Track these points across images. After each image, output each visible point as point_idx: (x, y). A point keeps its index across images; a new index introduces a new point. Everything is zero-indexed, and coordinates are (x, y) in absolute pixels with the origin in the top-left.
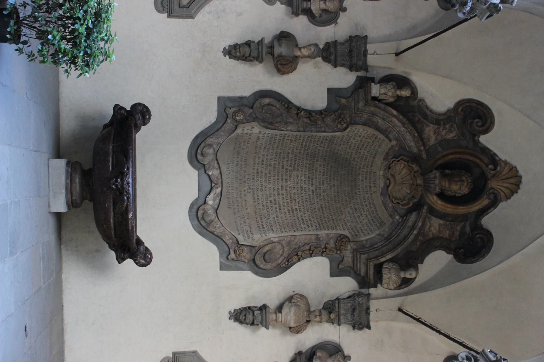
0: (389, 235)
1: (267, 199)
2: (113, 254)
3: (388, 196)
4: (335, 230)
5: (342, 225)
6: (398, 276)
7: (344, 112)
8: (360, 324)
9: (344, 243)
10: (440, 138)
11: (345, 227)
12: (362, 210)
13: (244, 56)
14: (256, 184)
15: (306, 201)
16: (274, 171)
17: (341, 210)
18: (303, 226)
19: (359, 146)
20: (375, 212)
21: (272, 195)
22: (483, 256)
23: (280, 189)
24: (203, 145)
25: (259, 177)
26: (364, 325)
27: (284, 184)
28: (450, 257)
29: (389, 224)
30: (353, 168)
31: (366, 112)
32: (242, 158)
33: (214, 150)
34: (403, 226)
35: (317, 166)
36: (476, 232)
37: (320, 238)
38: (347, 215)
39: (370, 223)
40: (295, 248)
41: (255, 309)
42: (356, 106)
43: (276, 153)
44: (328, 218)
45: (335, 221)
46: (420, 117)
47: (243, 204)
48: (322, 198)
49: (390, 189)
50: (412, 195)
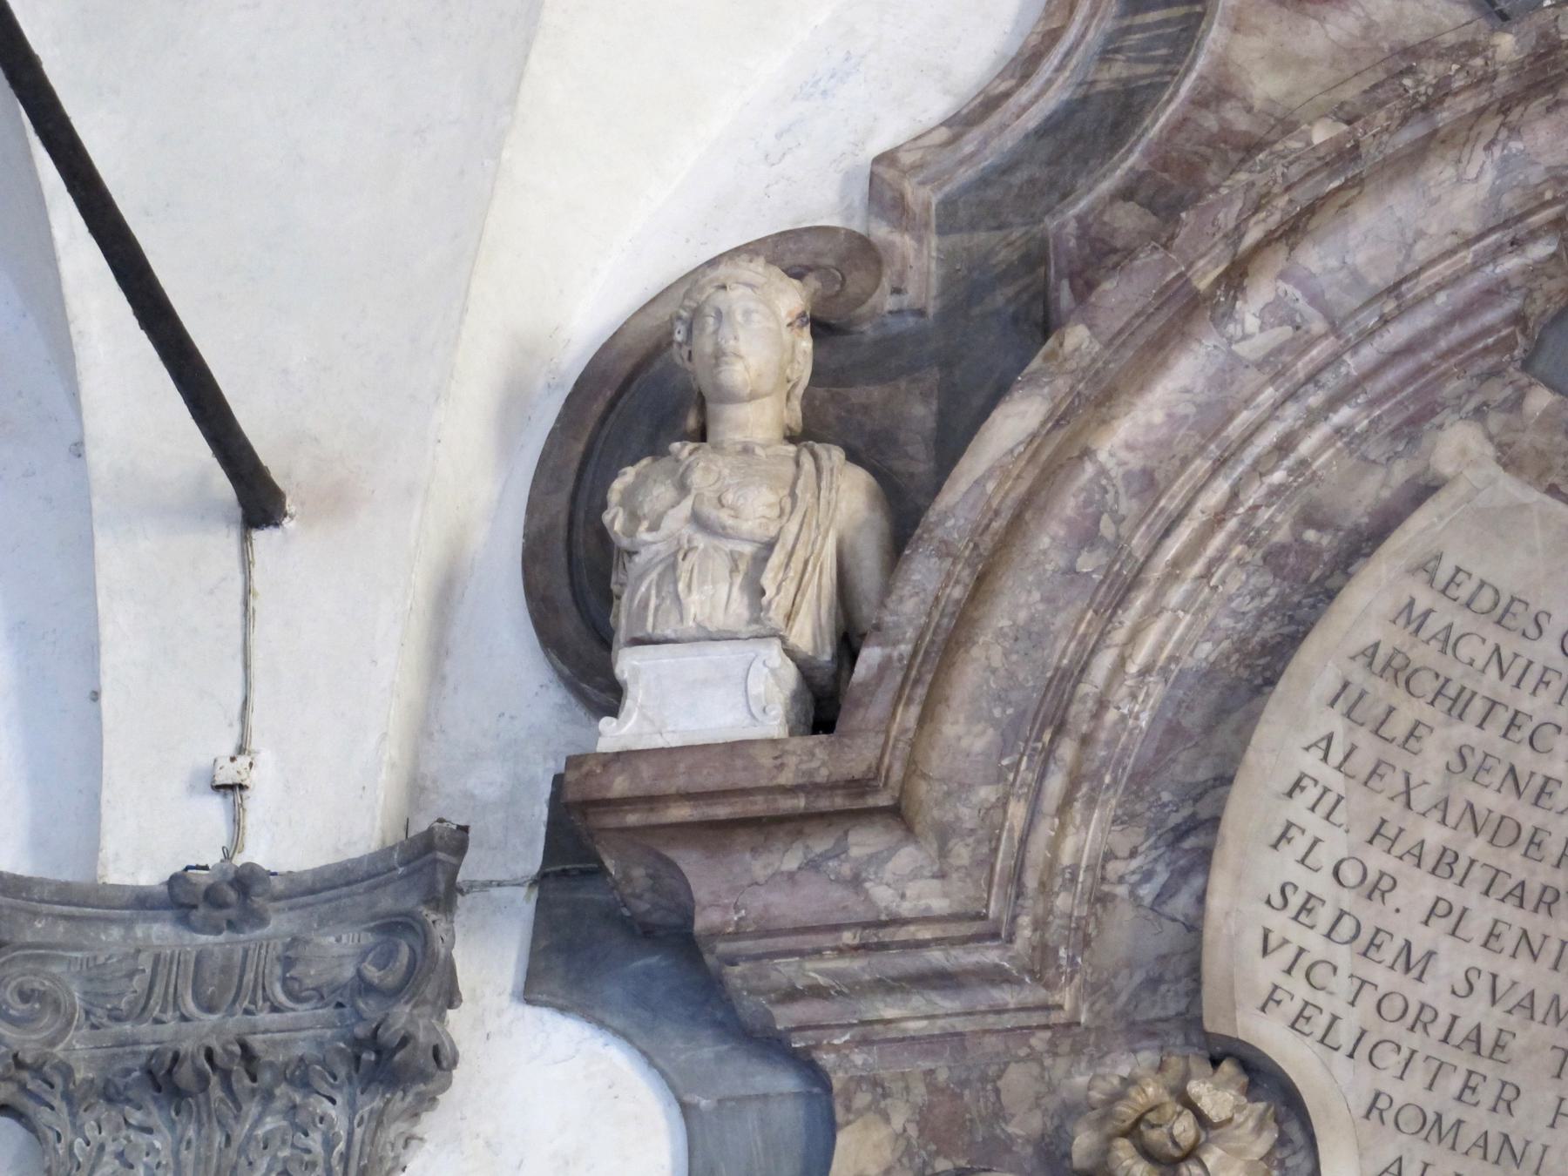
19: (1518, 895)
31: (1017, 812)
42: (936, 957)
46: (1106, 186)
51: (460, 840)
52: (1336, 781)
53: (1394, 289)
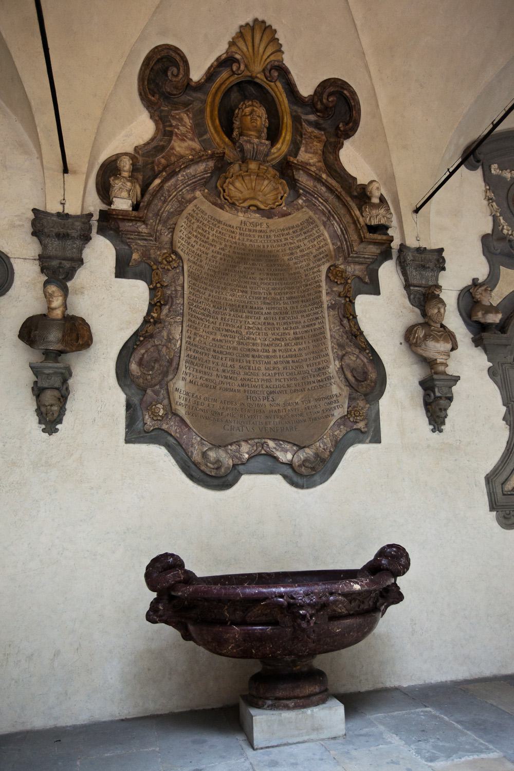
1: (282, 374)
2: (392, 609)
3: (273, 210)
4: (321, 283)
5: (314, 273)
10: (190, 134)
11: (315, 270)
12: (292, 246)
13: (59, 399)
14: (261, 389)
15: (284, 318)
18: (317, 326)
21: (276, 366)
22: (353, 93)
23: (268, 354)
25: (248, 382)
27: (260, 348)
28: (347, 143)
29: (311, 213)
30: (234, 252)
32: (222, 407)
33: (210, 449)
35: (233, 300)
36: (319, 103)
37: (331, 303)
38: (299, 265)
40: (347, 338)
42: (146, 237)
48: (279, 297)
49: (262, 207)
52: (186, 226)
53: (194, 176)
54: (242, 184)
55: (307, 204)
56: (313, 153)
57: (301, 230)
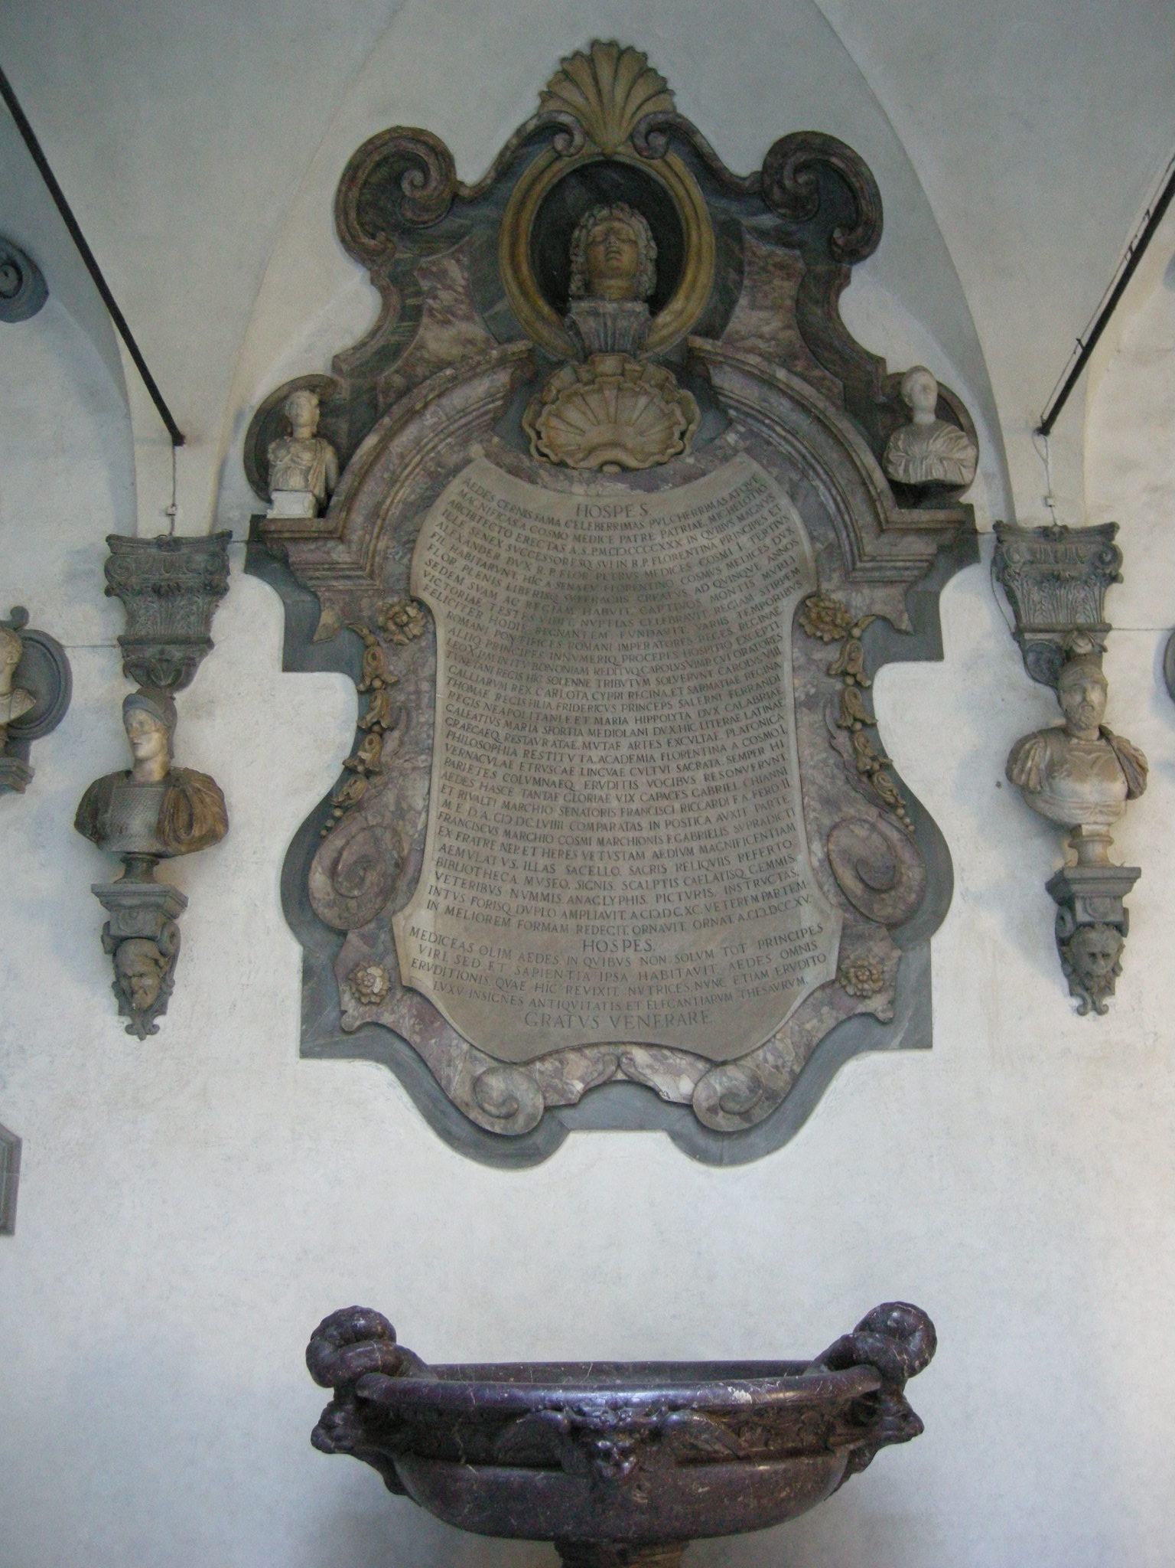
0: (793, 464)
2: (888, 1456)
3: (660, 470)
5: (762, 619)
6: (932, 430)
7: (366, 613)
8: (1101, 558)
9: (823, 614)
11: (767, 610)
12: (708, 553)
13: (156, 962)
14: (619, 922)
15: (679, 742)
16: (572, 855)
17: (707, 623)
18: (768, 755)
19: (485, 565)
20: (713, 512)
21: (657, 862)
22: (855, 161)
23: (637, 834)
24: (475, 1115)
25: (590, 907)
26: (1103, 544)
28: (860, 274)
29: (756, 466)
30: (560, 585)
31: (367, 537)
32: (522, 970)
33: (490, 1071)
34: (760, 417)
35: (554, 705)
36: (776, 190)
37: (807, 694)
38: (725, 602)
39: (752, 526)
40: (847, 780)
41: (1068, 917)
43: (506, 848)
44: (736, 668)
45: (749, 644)
46: (392, 369)
47: (690, 966)
48: (668, 689)
49: (632, 463)
50: (656, 391)
51: (230, 534)
52: (443, 534)
53: (463, 411)
54: (584, 413)
55: (748, 443)
56: (772, 308)
57: (734, 509)
